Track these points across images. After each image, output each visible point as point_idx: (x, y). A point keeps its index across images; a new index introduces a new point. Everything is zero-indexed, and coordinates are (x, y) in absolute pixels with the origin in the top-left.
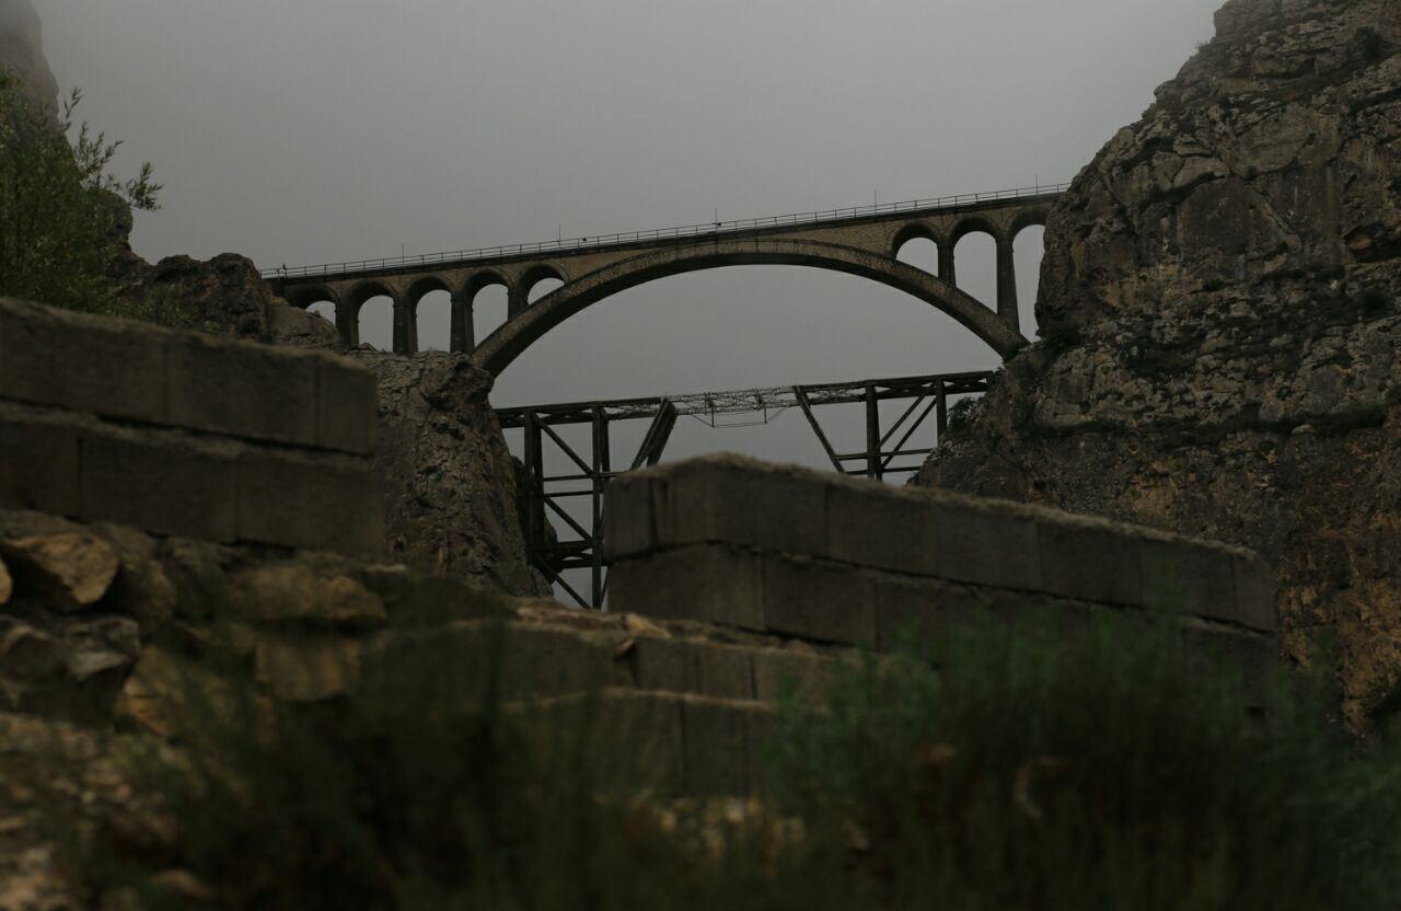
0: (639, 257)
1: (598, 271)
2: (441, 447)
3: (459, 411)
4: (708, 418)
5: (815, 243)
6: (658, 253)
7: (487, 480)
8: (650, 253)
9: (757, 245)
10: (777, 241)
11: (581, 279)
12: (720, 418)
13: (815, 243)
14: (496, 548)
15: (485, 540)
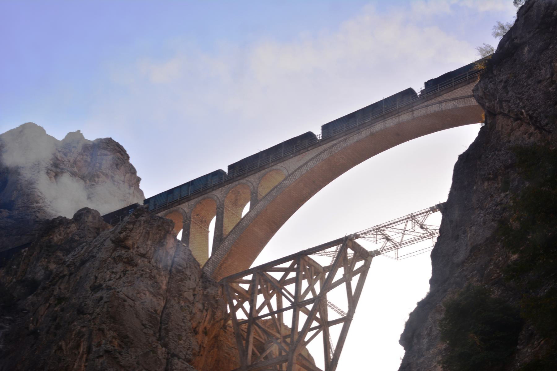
0: (333, 146)
1: (306, 163)
2: (113, 272)
3: (138, 247)
4: (392, 253)
5: (454, 99)
6: (346, 139)
7: (154, 296)
8: (341, 141)
9: (413, 114)
10: (427, 106)
11: (296, 171)
12: (402, 251)
13: (454, 99)
14: (126, 337)
15: (115, 331)
